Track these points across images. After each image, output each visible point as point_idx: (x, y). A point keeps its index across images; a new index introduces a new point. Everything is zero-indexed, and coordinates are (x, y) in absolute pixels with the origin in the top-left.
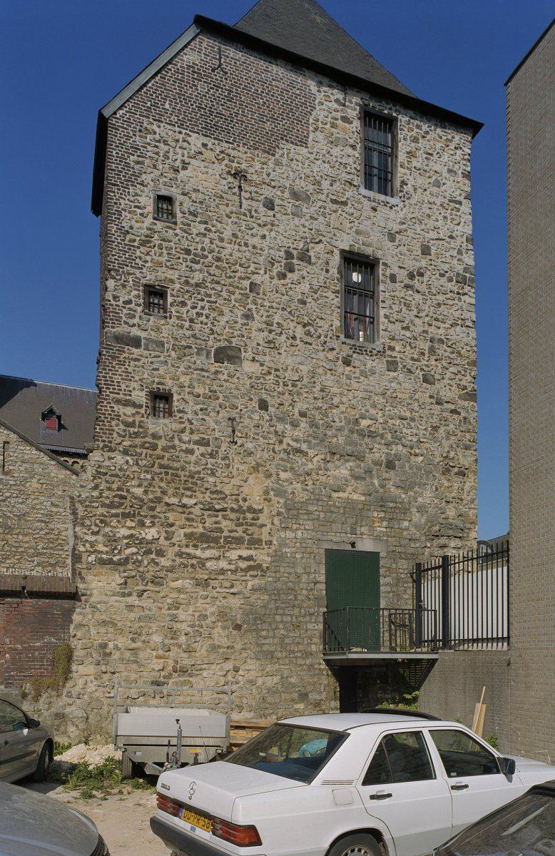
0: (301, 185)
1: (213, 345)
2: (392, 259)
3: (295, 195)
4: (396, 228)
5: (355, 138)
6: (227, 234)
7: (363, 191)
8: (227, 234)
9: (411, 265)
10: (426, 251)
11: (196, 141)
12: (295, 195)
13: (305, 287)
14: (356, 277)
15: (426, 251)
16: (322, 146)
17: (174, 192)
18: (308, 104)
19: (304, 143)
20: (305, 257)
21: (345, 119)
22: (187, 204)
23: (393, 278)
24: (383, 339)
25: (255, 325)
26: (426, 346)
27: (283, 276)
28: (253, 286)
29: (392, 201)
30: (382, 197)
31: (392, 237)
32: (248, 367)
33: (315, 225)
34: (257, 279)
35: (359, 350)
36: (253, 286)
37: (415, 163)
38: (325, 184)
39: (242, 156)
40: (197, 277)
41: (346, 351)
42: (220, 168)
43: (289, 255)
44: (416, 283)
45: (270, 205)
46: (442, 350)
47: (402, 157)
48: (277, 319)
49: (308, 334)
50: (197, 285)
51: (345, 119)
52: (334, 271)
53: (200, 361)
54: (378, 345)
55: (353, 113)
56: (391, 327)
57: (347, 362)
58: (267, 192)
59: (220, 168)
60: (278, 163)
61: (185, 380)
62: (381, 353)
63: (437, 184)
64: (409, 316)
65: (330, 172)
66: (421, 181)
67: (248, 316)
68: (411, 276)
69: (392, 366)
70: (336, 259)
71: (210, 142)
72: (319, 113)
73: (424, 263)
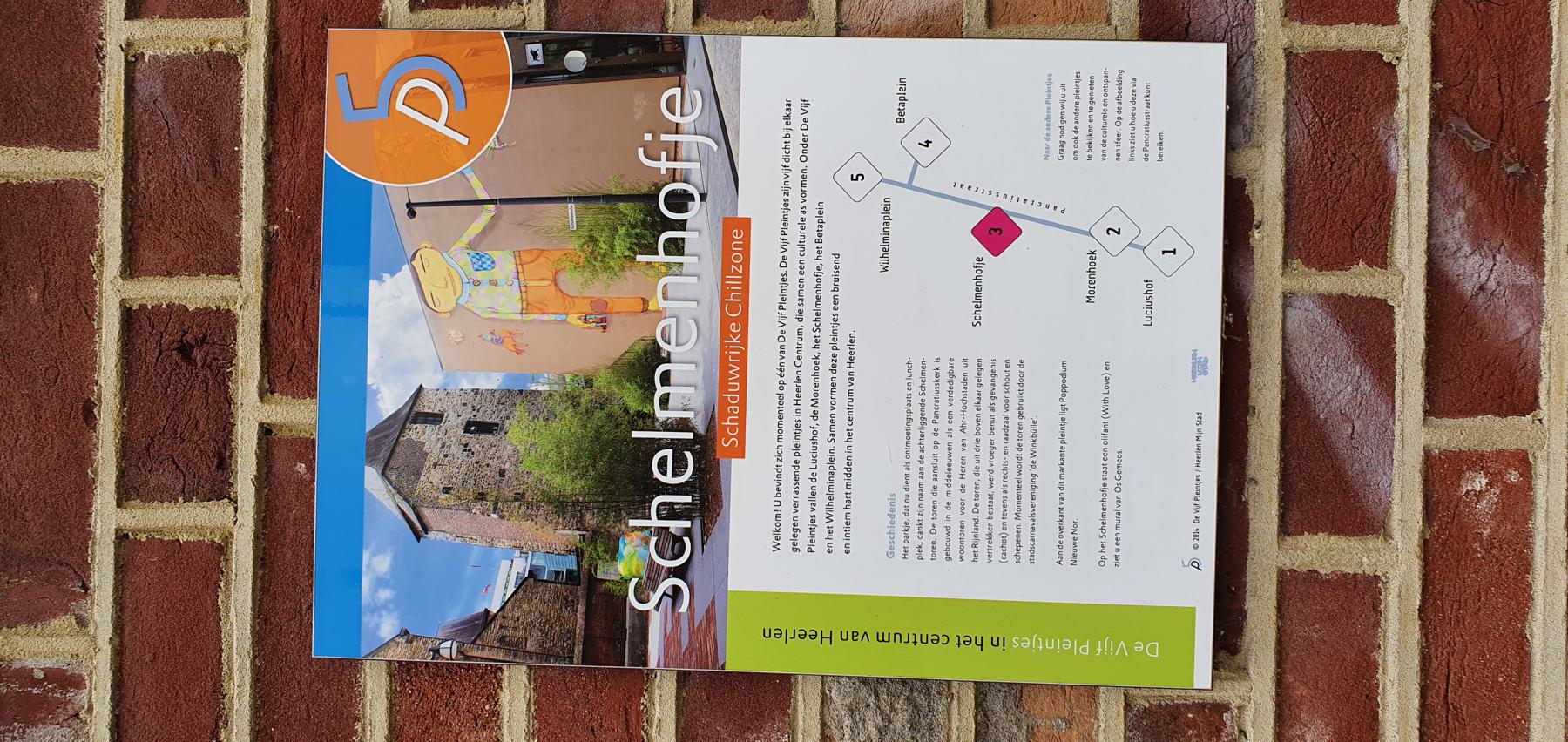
0: (439, 445)
1: (498, 478)
2: (468, 415)
3: (443, 447)
4: (456, 414)
5: (423, 426)
6: (457, 471)
7: (442, 424)
8: (457, 471)
9: (470, 409)
10: (465, 405)
11: (422, 478)
12: (443, 447)
13: (477, 446)
14: (473, 428)
15: (465, 405)
16: (425, 436)
17: (441, 487)
18: (410, 440)
19: (424, 443)
20: (466, 445)
21: (416, 428)
22: (445, 483)
23: (475, 416)
24: (497, 420)
25: (490, 462)
26: (501, 406)
27: (473, 453)
28: (476, 463)
29: (446, 414)
30: (444, 419)
31: (459, 416)
32: (507, 466)
33: (454, 441)
34: (474, 461)
35: (502, 429)
36: (476, 463)
37: (432, 407)
38: (439, 437)
39: (427, 463)
40: (473, 482)
41: (502, 433)
42: (432, 471)
43: (465, 450)
44: (477, 409)
45: (446, 456)
46: (503, 400)
47: (430, 411)
48: (489, 456)
49: (495, 446)
50: (476, 481)
51: (416, 428)
52: (472, 436)
53: (504, 482)
54: (500, 422)
55: (414, 426)
56: (494, 417)
57: (506, 433)
58: (442, 456)
59: (432, 471)
60: (431, 452)
61: (511, 488)
62: (503, 421)
63: (440, 400)
64: (489, 411)
65: (434, 436)
66: (439, 404)
67: (488, 465)
68: (474, 410)
69: (508, 418)
70: (467, 435)
71: (423, 474)
72: (413, 437)
73: (470, 406)
